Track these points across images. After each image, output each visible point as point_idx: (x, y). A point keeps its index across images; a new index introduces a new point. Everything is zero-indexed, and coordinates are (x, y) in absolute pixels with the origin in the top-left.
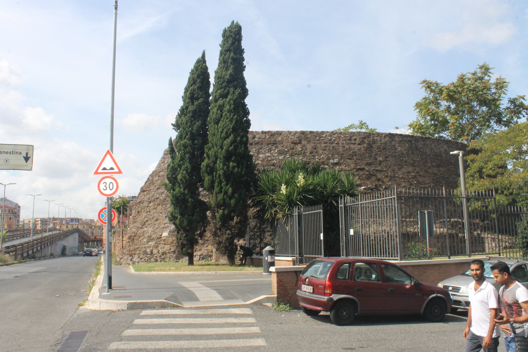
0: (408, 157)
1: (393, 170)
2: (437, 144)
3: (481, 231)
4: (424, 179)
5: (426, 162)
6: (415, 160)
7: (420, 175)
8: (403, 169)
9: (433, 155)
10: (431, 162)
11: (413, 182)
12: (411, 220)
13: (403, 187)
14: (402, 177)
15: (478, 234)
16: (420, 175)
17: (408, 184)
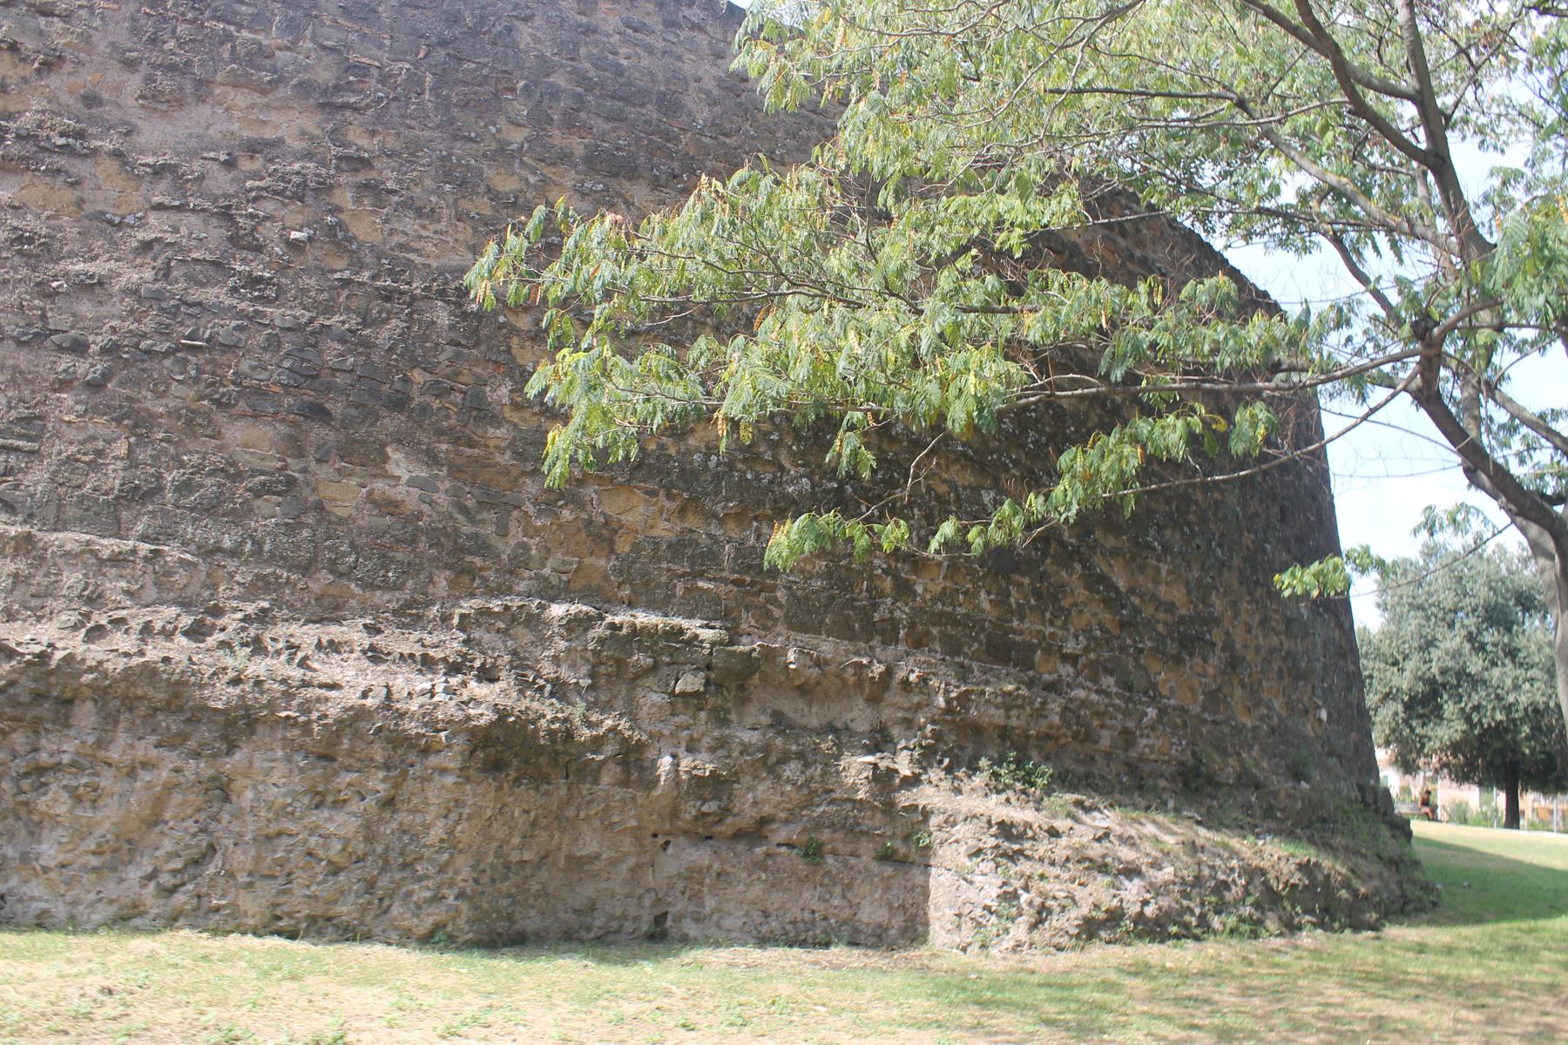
0: (292, 27)
1: (91, 100)
2: (655, 22)
3: (927, 757)
4: (409, 224)
5: (490, 106)
6: (362, 70)
7: (372, 189)
8: (205, 110)
9: (580, 78)
10: (540, 119)
11: (270, 232)
12: (109, 546)
13: (146, 246)
14: (159, 171)
15: (883, 780)
16: (372, 189)
17: (216, 233)
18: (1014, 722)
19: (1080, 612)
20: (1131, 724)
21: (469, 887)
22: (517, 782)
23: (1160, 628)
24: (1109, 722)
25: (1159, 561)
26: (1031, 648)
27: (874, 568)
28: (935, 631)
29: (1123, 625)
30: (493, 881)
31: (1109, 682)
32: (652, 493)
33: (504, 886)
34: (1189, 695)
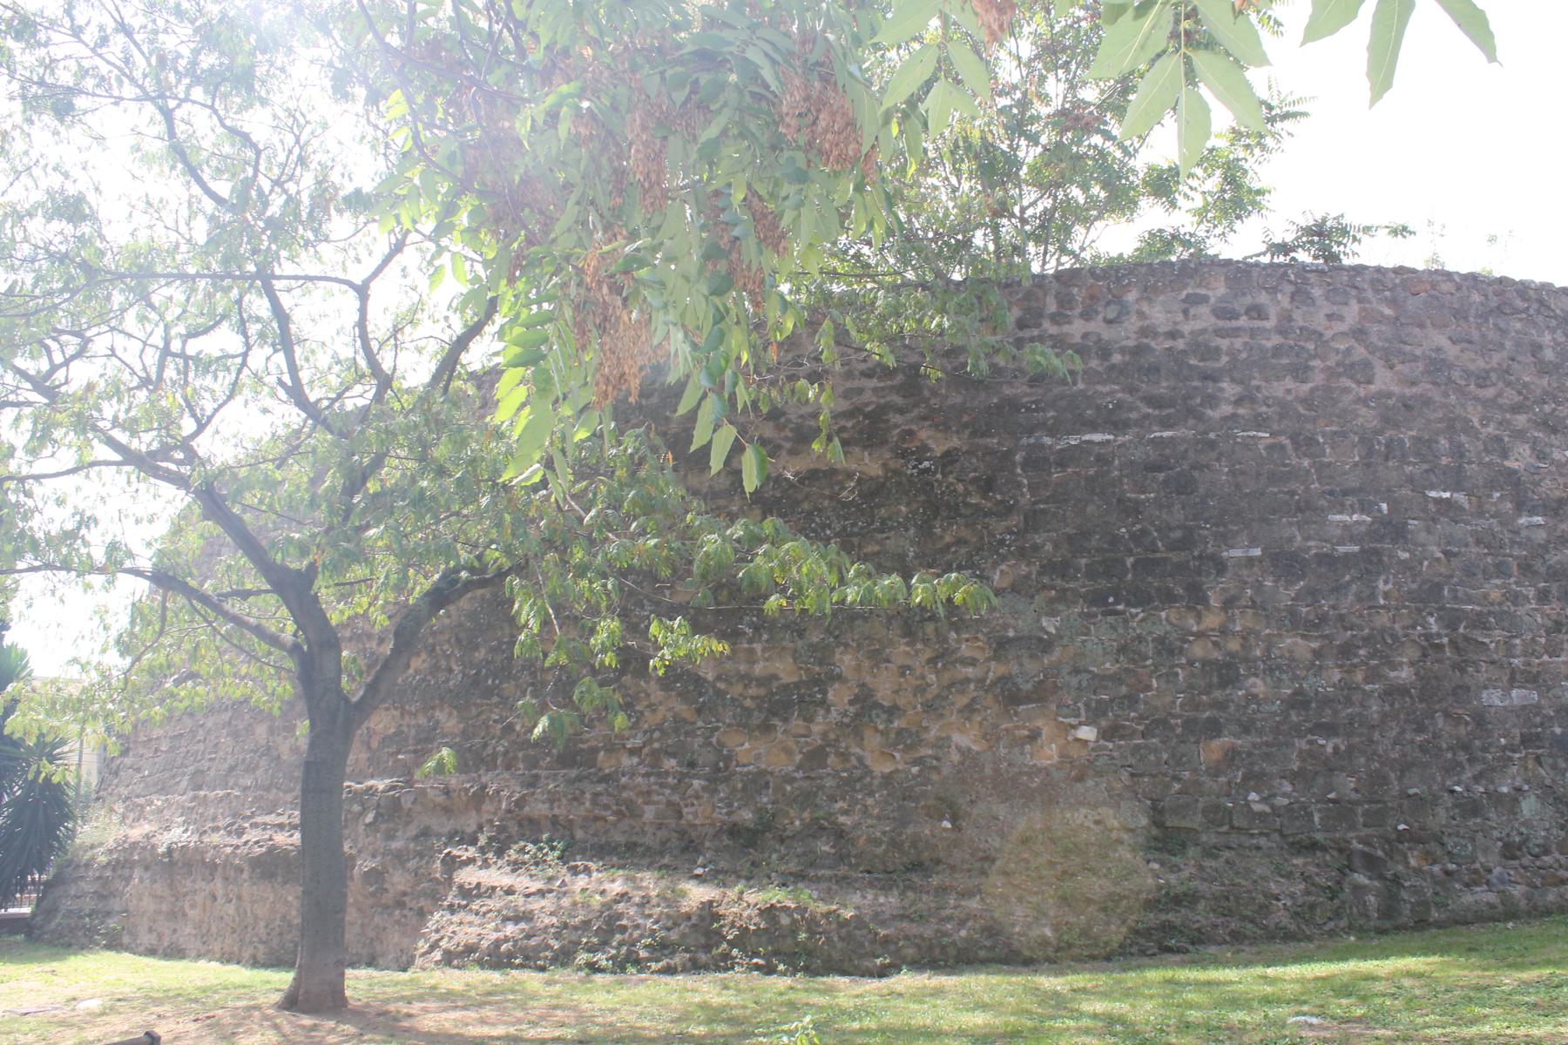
18: (557, 811)
19: (654, 711)
20: (676, 798)
21: (264, 938)
22: (285, 883)
23: (748, 703)
24: (655, 798)
25: (751, 641)
26: (595, 750)
27: (489, 719)
28: (520, 755)
29: (699, 711)
30: (281, 934)
31: (670, 764)
32: (387, 709)
33: (289, 937)
34: (783, 756)
